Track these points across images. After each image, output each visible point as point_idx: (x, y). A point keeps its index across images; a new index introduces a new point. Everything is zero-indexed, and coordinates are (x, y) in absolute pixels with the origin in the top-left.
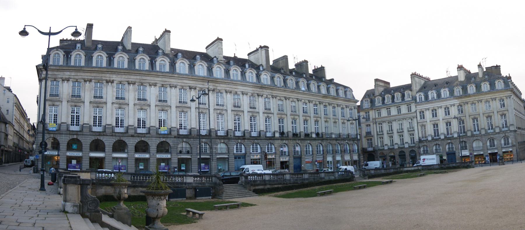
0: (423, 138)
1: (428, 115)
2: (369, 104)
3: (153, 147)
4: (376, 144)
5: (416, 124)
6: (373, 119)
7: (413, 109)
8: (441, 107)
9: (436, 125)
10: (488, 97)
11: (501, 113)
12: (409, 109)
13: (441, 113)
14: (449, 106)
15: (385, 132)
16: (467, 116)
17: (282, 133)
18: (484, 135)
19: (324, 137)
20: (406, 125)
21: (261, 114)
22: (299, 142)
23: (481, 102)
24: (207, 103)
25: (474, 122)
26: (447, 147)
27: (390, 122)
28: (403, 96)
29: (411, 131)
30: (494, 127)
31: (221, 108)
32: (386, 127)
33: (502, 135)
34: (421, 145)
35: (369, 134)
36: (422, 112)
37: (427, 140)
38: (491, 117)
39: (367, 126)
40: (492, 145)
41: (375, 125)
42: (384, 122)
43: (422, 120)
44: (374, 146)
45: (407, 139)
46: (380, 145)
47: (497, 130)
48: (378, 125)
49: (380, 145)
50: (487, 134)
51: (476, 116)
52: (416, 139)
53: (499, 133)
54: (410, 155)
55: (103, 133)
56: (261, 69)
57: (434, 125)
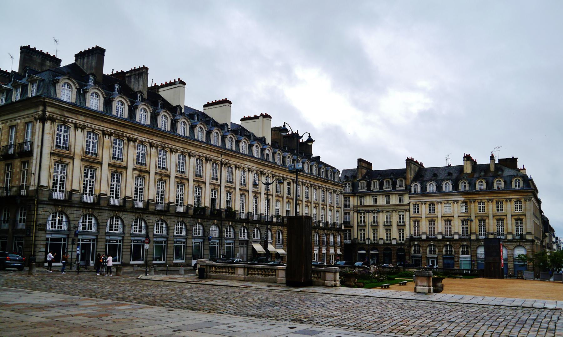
0: (415, 235)
1: (424, 210)
2: (351, 188)
6: (354, 207)
11: (516, 217)
12: (401, 200)
20: (395, 218)
23: (492, 202)
26: (444, 249)
28: (394, 185)
29: (401, 227)
30: (505, 233)
36: (416, 205)
38: (502, 220)
41: (356, 214)
42: (368, 212)
44: (352, 238)
46: (359, 238)
47: (510, 237)
49: (359, 238)
52: (407, 235)
54: (397, 254)
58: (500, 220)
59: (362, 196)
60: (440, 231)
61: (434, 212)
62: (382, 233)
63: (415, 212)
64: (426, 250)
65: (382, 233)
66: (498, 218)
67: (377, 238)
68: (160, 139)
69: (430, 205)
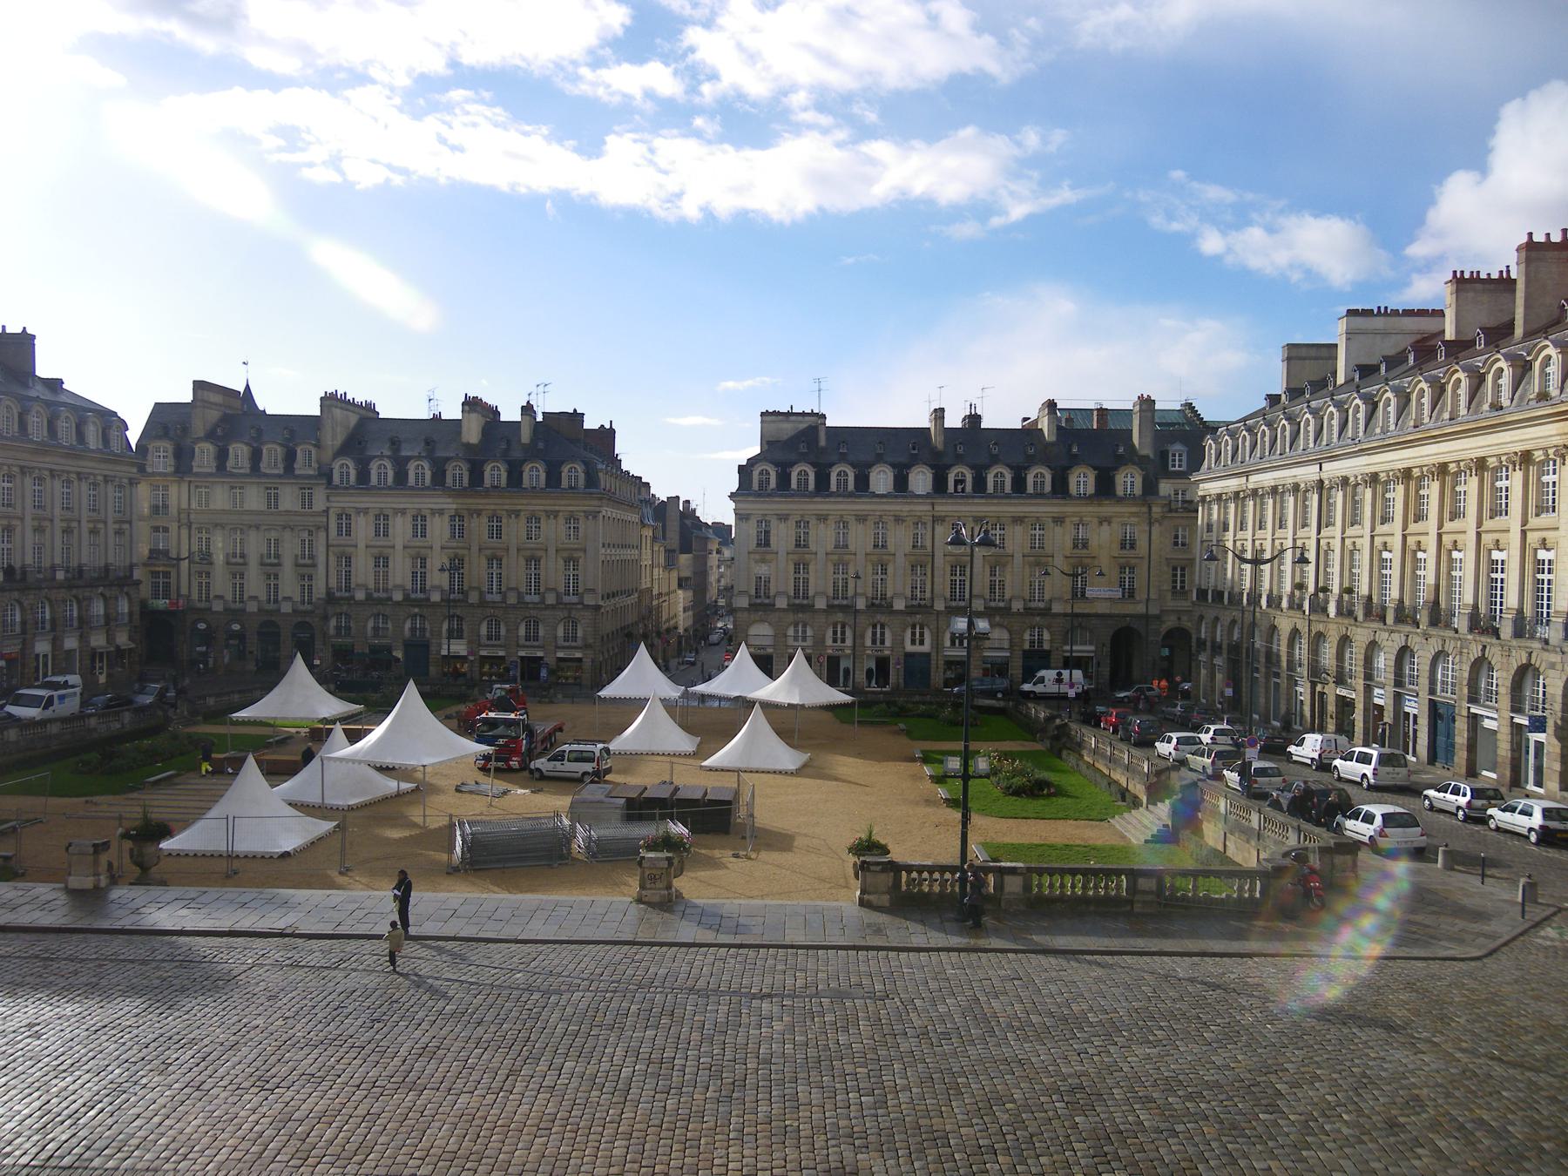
1: (363, 529)
4: (184, 591)
7: (319, 503)
8: (403, 512)
9: (382, 561)
10: (538, 506)
11: (566, 554)
12: (307, 501)
13: (401, 529)
14: (427, 513)
16: (475, 548)
18: (514, 607)
25: (490, 566)
26: (408, 625)
29: (305, 570)
33: (561, 614)
36: (345, 518)
37: (353, 598)
38: (537, 561)
39: (156, 529)
40: (532, 636)
41: (184, 532)
42: (222, 526)
43: (344, 540)
44: (174, 596)
45: (289, 586)
46: (195, 596)
48: (195, 535)
49: (195, 596)
51: (499, 553)
52: (319, 590)
53: (553, 607)
54: (294, 635)
57: (377, 559)
60: (398, 581)
61: (386, 534)
63: (340, 533)
64: (365, 627)
66: (528, 553)
67: (242, 595)
69: (377, 517)
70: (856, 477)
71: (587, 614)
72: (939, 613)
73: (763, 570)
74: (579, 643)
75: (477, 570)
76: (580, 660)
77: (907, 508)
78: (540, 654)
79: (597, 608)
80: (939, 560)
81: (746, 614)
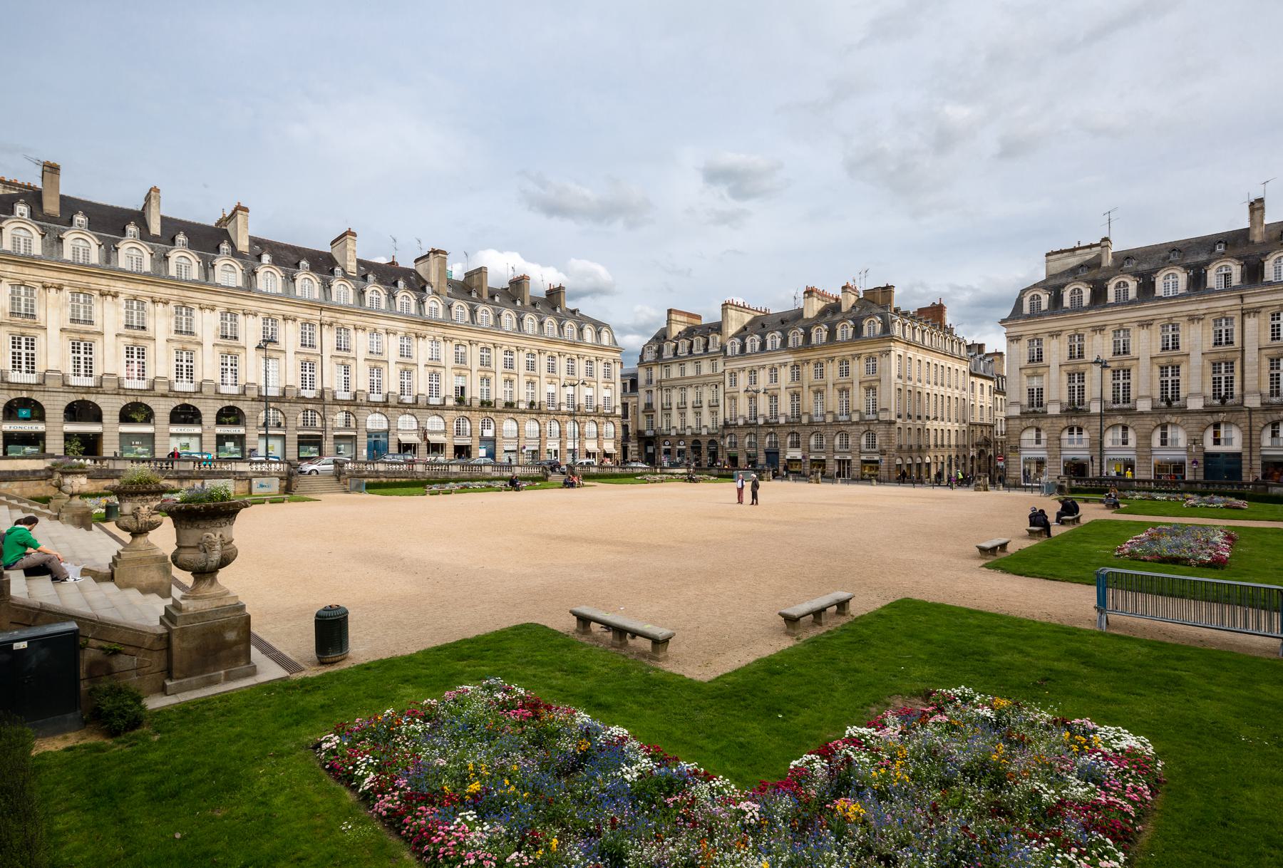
1: (743, 380)
3: (209, 416)
5: (721, 395)
7: (720, 370)
10: (847, 352)
11: (866, 385)
12: (714, 367)
13: (763, 379)
15: (674, 406)
16: (806, 387)
17: (460, 401)
18: (831, 424)
19: (544, 409)
21: (421, 367)
22: (492, 415)
24: (318, 343)
26: (768, 440)
27: (683, 388)
31: (345, 354)
32: (676, 397)
33: (863, 428)
34: (726, 432)
35: (649, 406)
38: (847, 391)
47: (855, 418)
50: (836, 422)
52: (721, 422)
53: (857, 423)
55: (98, 389)
56: (428, 289)
58: (844, 391)
59: (667, 365)
62: (691, 420)
65: (691, 420)
66: (840, 387)
68: (175, 292)
70: (1139, 286)
71: (882, 427)
72: (1251, 410)
73: (1035, 383)
74: (877, 449)
75: (808, 402)
76: (876, 462)
77: (1204, 306)
78: (849, 457)
79: (892, 423)
80: (1251, 355)
81: (1018, 422)
